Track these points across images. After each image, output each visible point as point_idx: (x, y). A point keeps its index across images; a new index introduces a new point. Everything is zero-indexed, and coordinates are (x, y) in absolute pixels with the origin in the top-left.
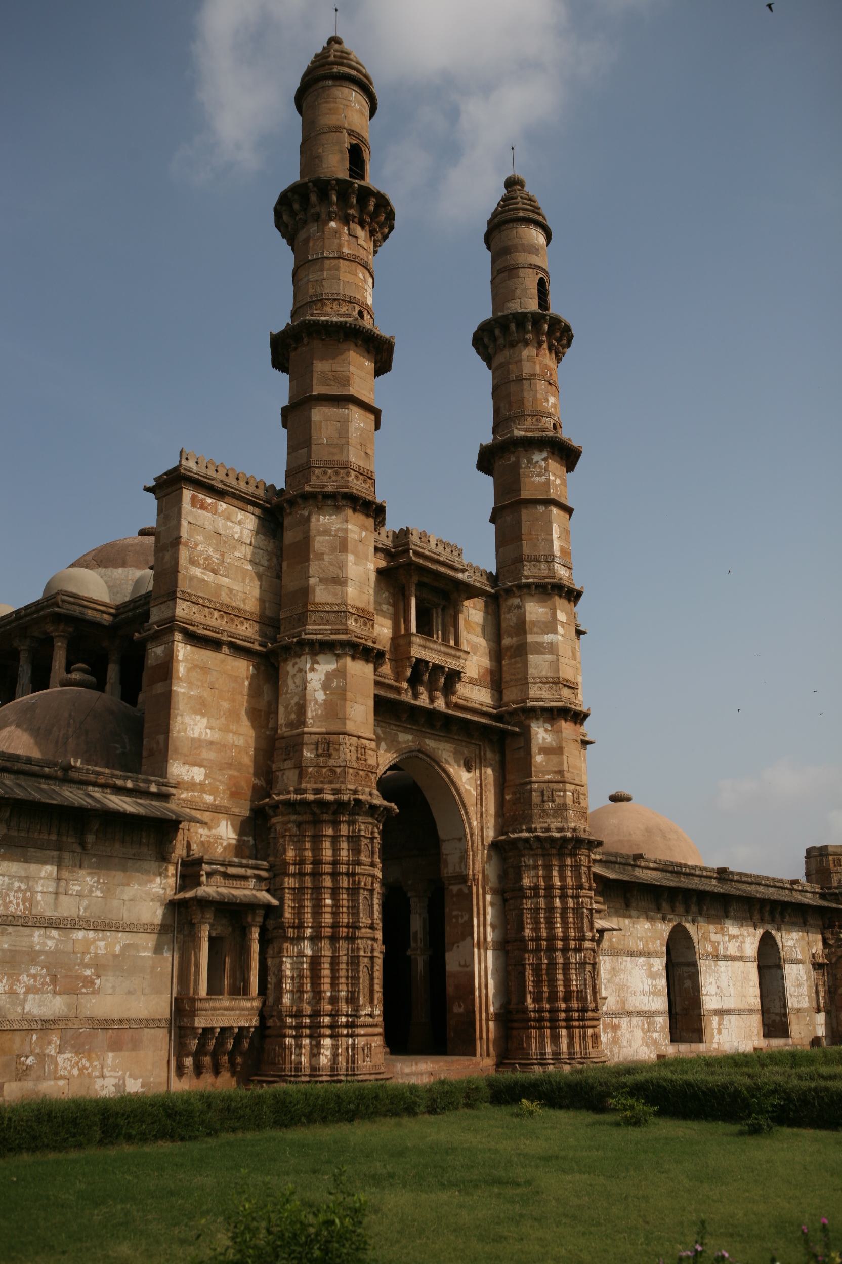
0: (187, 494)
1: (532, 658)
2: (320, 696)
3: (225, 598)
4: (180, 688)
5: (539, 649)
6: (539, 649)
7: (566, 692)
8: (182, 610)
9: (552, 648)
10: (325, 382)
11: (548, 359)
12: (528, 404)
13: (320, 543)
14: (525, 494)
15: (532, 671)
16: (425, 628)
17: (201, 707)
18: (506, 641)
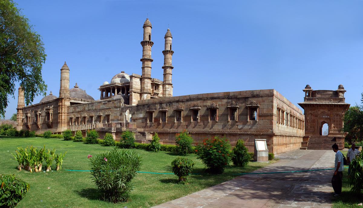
0: (133, 78)
1: (166, 92)
2: (145, 98)
3: (136, 88)
4: (133, 97)
5: (167, 91)
6: (167, 91)
7: (170, 95)
8: (133, 89)
9: (169, 91)
10: (146, 65)
11: (171, 56)
12: (168, 61)
13: (146, 82)
14: (167, 73)
15: (166, 93)
16: (155, 89)
17: (135, 99)
18: (164, 89)
